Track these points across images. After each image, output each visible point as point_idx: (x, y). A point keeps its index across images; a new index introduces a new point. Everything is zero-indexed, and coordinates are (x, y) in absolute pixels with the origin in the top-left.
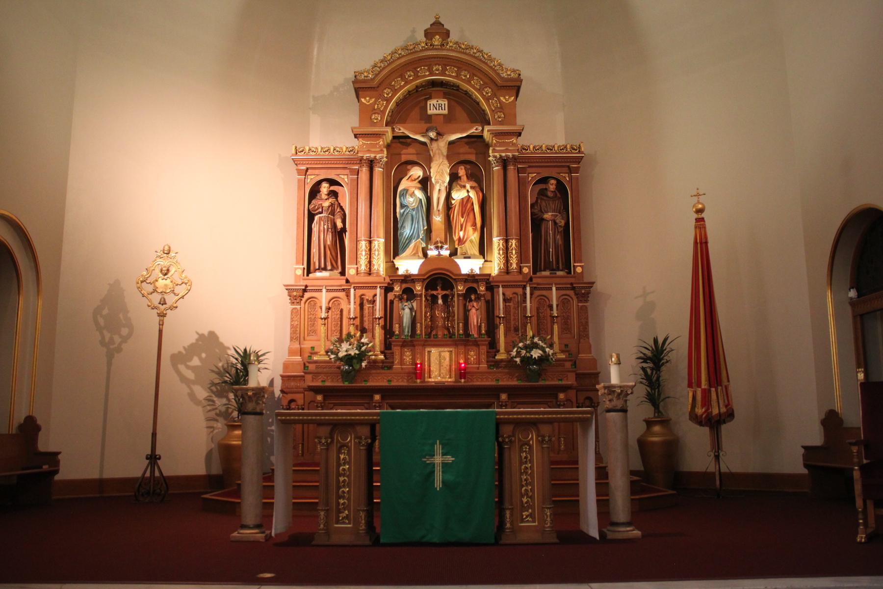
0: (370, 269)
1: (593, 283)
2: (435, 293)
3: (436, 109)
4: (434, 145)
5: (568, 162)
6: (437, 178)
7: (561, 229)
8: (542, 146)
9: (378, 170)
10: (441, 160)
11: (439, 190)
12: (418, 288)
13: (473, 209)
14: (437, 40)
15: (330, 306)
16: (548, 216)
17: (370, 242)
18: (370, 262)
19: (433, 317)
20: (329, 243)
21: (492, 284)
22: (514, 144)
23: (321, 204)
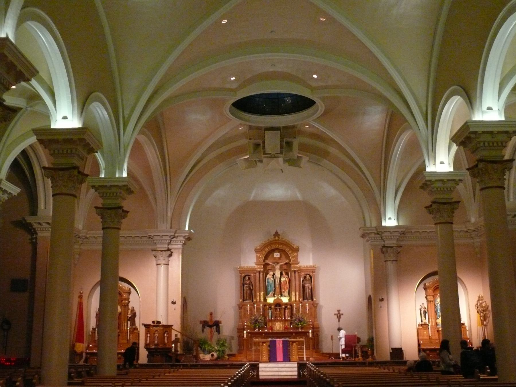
2: (277, 308)
7: (310, 289)
9: (261, 274)
12: (273, 307)
14: (277, 238)
16: (307, 285)
17: (260, 293)
19: (276, 314)
20: (249, 292)
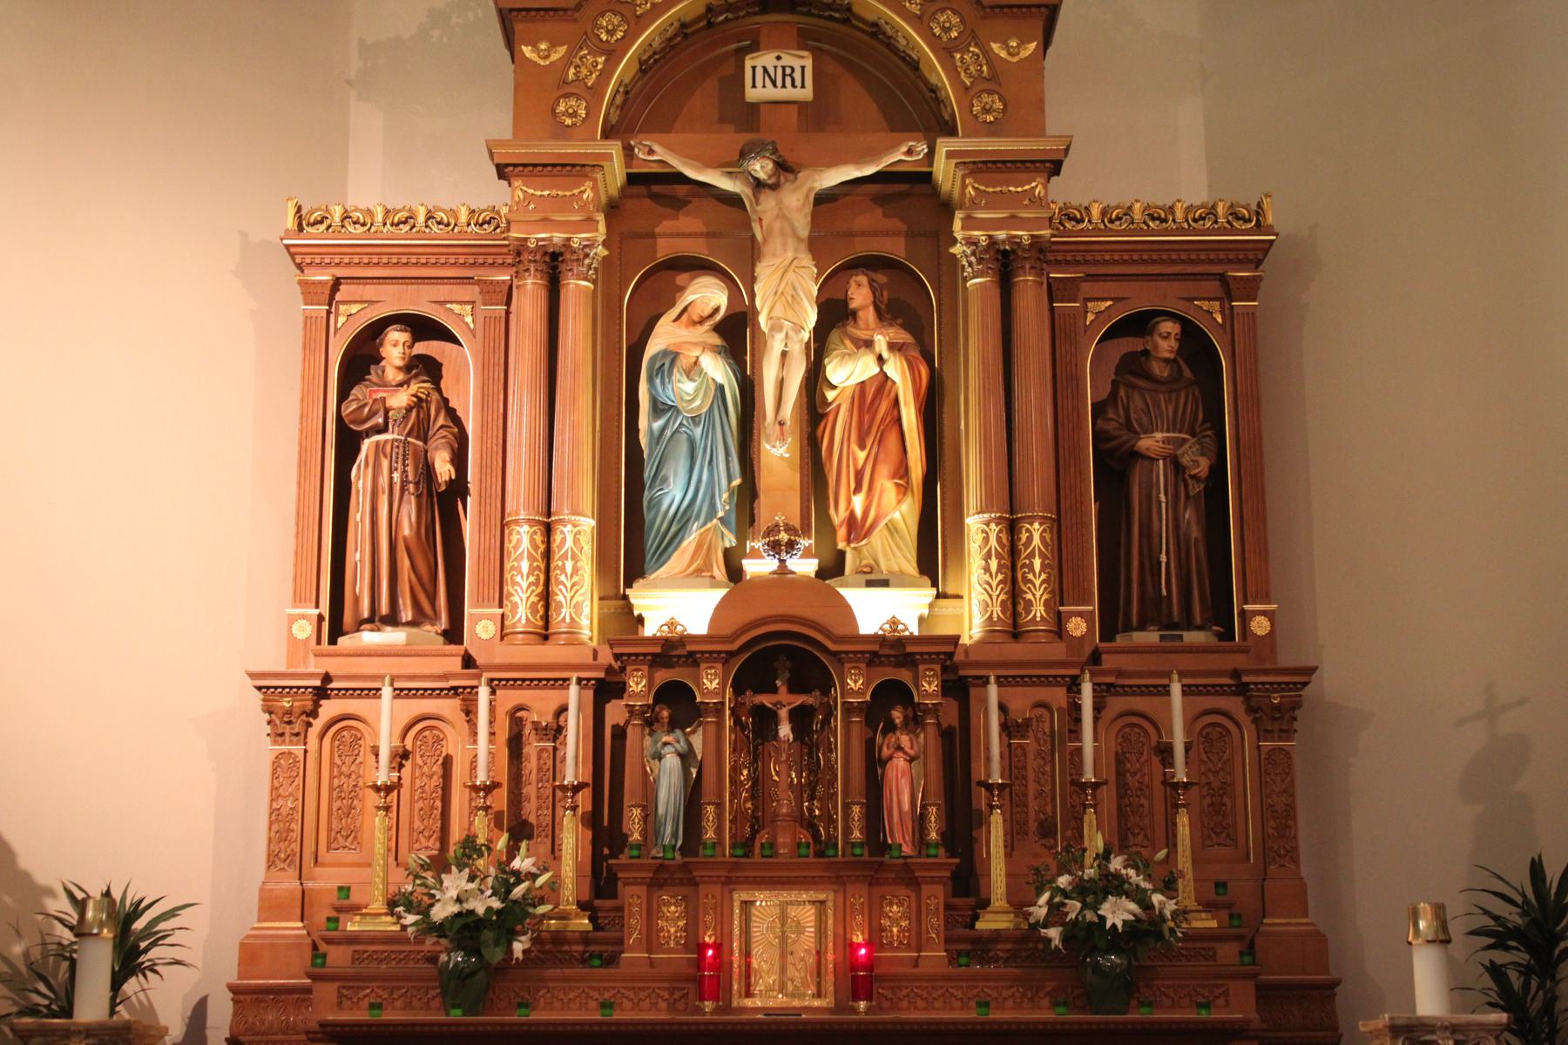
0: (546, 618)
1: (1311, 671)
2: (766, 700)
3: (774, 83)
4: (768, 204)
5: (1220, 262)
6: (778, 312)
7: (1196, 489)
8: (1130, 208)
9: (577, 287)
10: (790, 255)
11: (784, 354)
12: (710, 683)
13: (899, 420)
15: (409, 747)
16: (1153, 442)
17: (548, 530)
18: (546, 597)
19: (759, 785)
20: (406, 530)
21: (962, 673)
22: (1037, 202)
23: (384, 400)
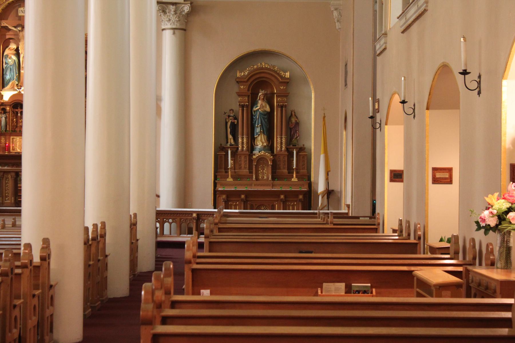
2: (17, 110)
3: (23, 13)
6: (22, 50)
12: (8, 109)
